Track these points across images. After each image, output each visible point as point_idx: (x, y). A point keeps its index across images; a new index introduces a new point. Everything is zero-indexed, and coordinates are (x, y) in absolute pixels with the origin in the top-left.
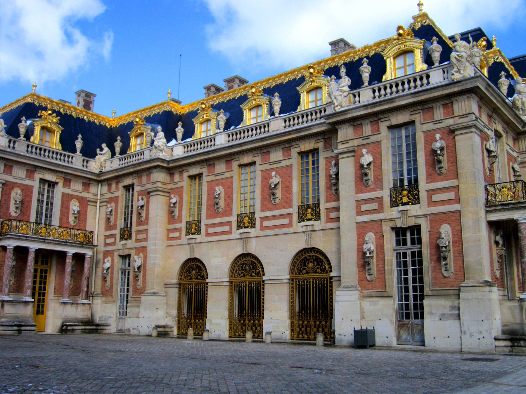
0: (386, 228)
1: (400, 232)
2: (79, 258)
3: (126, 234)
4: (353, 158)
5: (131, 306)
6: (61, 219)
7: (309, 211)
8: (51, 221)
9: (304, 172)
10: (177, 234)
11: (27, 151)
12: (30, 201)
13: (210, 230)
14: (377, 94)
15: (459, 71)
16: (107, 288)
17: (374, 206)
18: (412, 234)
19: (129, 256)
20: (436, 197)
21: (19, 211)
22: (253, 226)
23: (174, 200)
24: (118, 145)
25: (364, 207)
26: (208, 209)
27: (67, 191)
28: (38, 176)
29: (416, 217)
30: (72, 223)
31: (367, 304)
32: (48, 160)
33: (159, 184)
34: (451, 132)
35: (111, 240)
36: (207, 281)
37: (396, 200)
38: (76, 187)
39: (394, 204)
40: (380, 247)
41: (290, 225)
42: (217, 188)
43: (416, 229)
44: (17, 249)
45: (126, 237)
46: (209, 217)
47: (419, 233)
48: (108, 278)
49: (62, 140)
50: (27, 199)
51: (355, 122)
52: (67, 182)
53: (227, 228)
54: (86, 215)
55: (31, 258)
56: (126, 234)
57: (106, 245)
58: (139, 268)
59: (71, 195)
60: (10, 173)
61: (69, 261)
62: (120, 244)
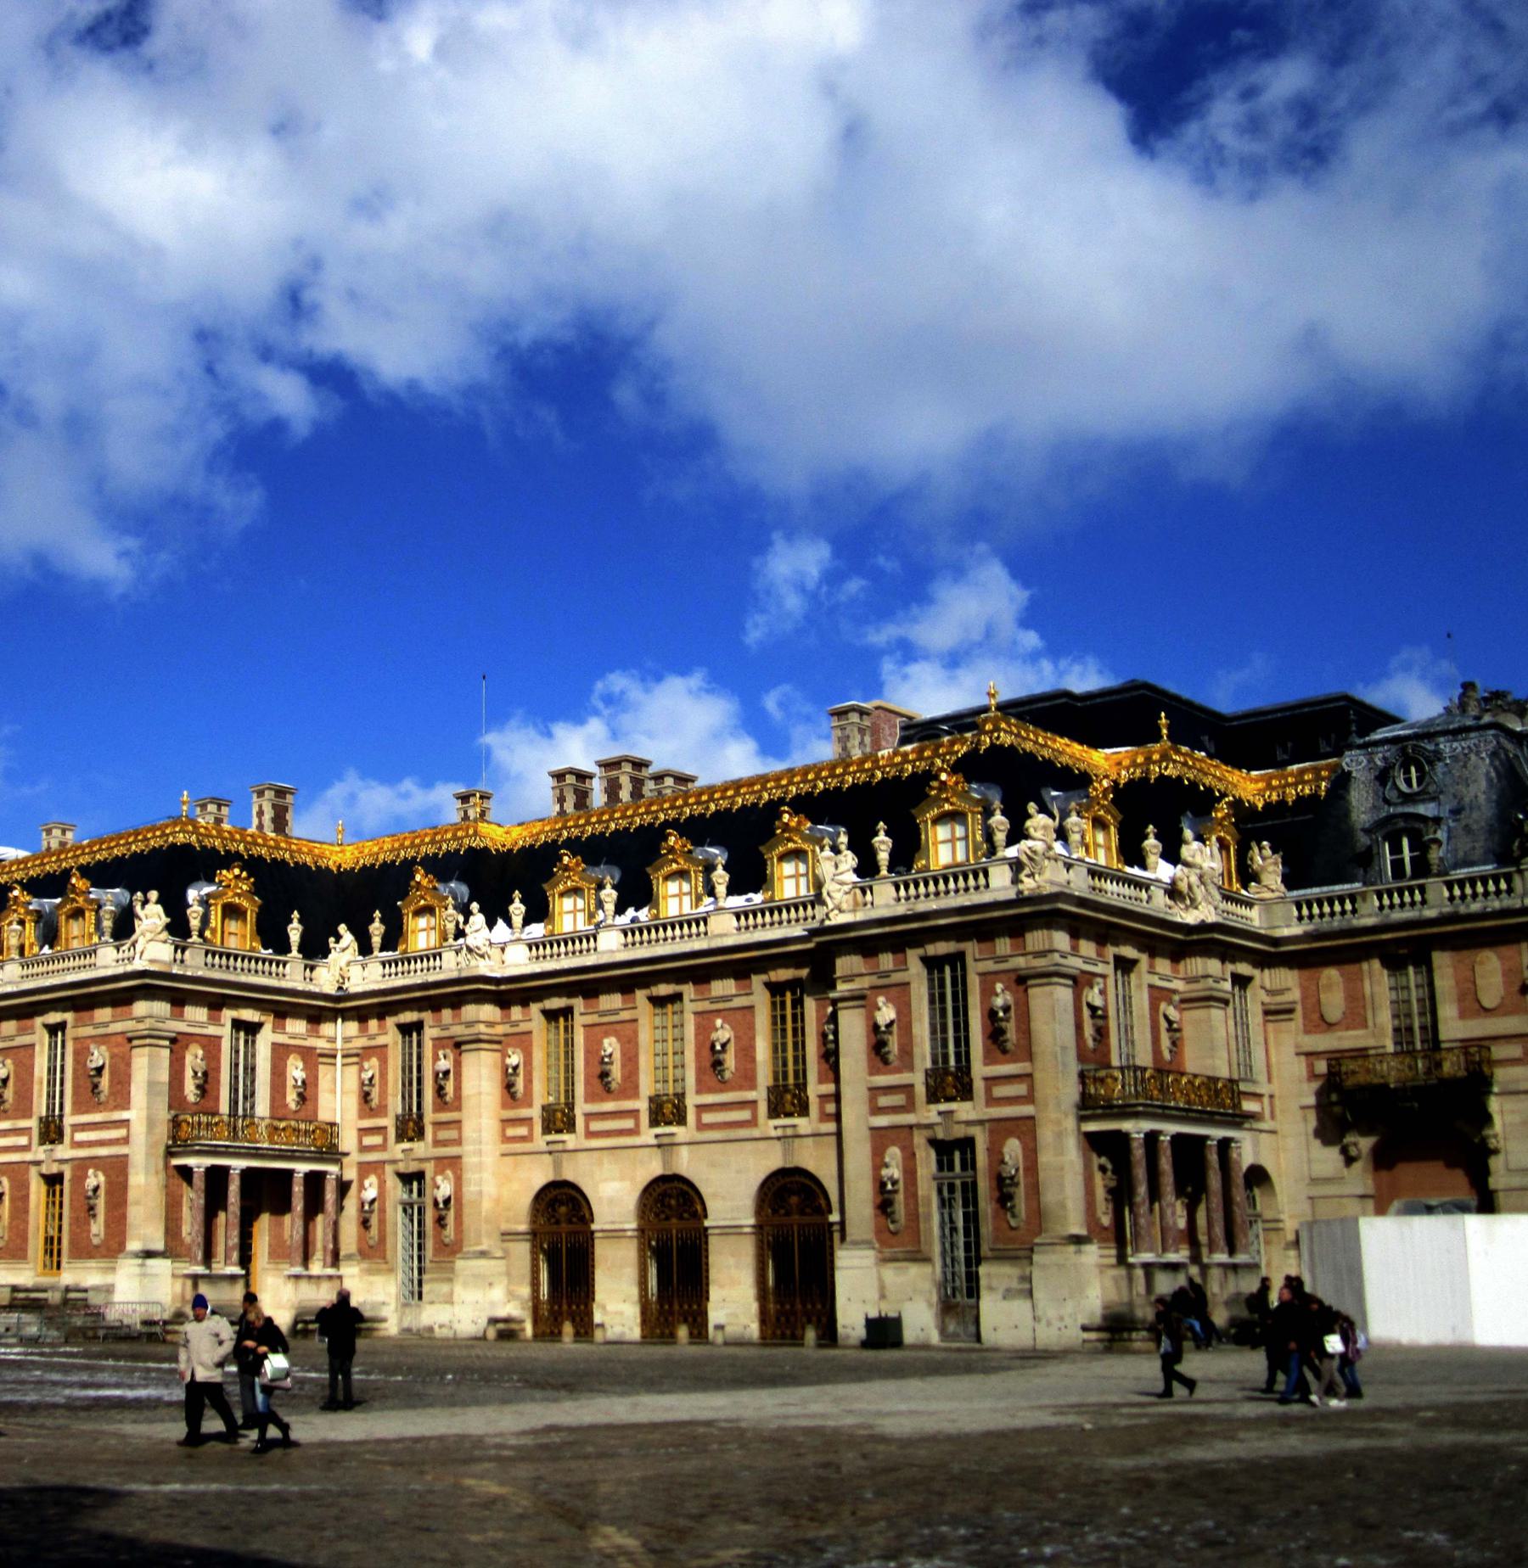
0: (919, 1139)
1: (943, 1149)
2: (315, 1182)
3: (410, 1128)
4: (862, 1011)
5: (432, 1280)
7: (787, 1099)
8: (252, 1107)
9: (778, 1021)
12: (218, 1069)
13: (596, 1126)
15: (1031, 875)
16: (371, 1242)
19: (419, 1176)
20: (1000, 1091)
22: (681, 1120)
24: (377, 929)
25: (884, 1101)
26: (587, 1083)
27: (281, 1039)
29: (968, 1123)
31: (890, 1273)
32: (243, 979)
33: (482, 1028)
34: (1022, 981)
35: (376, 1140)
40: (910, 1172)
41: (752, 1123)
42: (606, 1042)
43: (967, 1144)
45: (411, 1133)
48: (374, 1220)
50: (213, 1065)
53: (628, 1124)
54: (316, 1085)
55: (234, 1188)
58: (447, 1201)
60: (179, 1016)
61: (298, 1189)
62: (397, 1150)
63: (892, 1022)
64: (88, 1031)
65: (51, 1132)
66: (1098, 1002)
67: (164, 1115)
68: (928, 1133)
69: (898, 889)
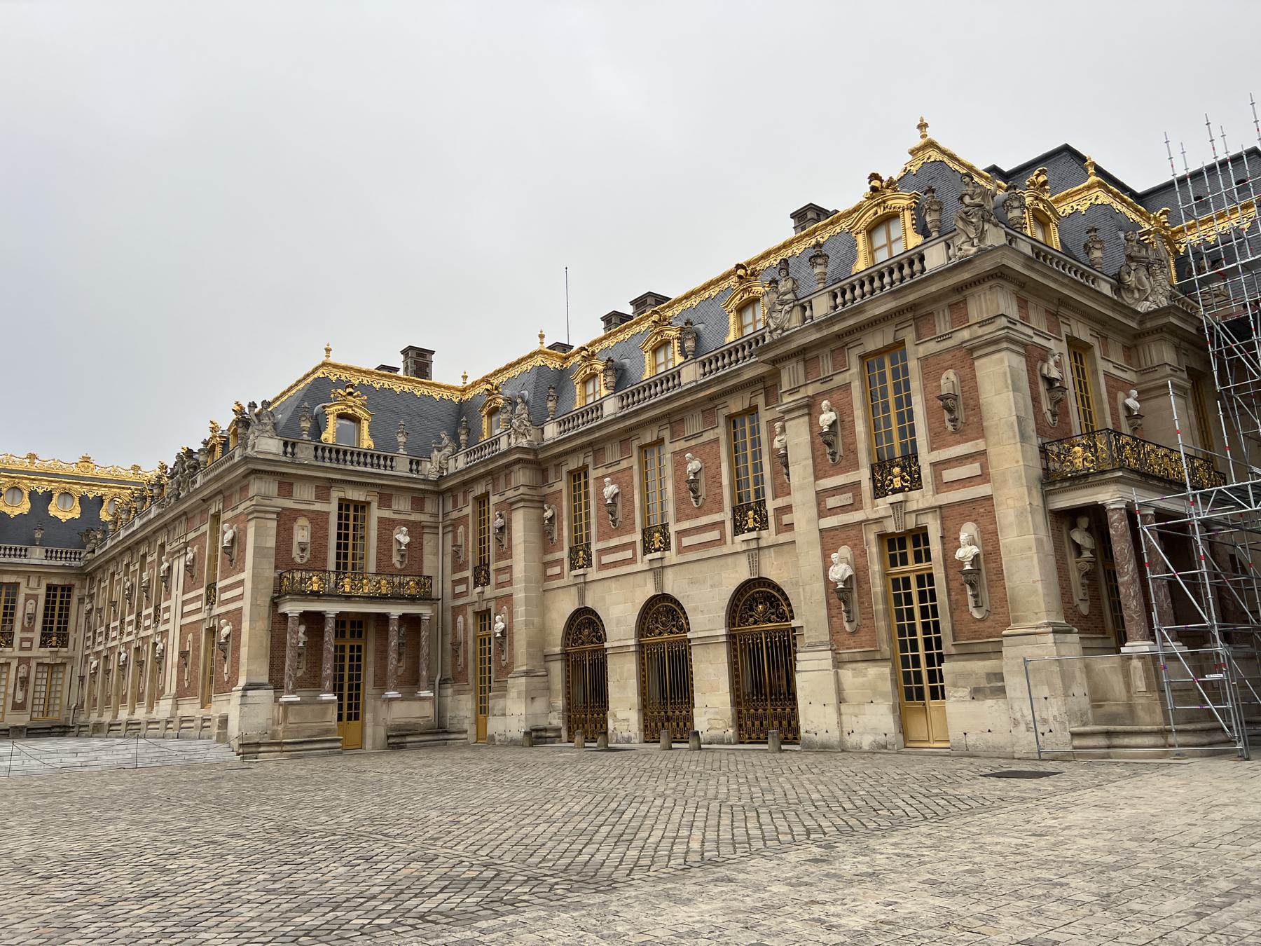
0: (871, 536)
2: (411, 622)
6: (379, 561)
10: (557, 570)
11: (316, 457)
12: (326, 537)
13: (606, 559)
14: (839, 300)
17: (845, 499)
18: (916, 544)
20: (949, 475)
21: (307, 555)
23: (548, 514)
25: (832, 502)
26: (599, 524)
27: (386, 514)
28: (336, 495)
29: (919, 512)
30: (398, 565)
32: (351, 468)
36: (606, 645)
37: (883, 486)
38: (402, 505)
39: (880, 491)
43: (920, 536)
44: (305, 617)
47: (927, 542)
49: (372, 435)
50: (320, 533)
51: (805, 354)
52: (385, 501)
53: (628, 554)
54: (421, 550)
55: (330, 627)
56: (481, 575)
57: (456, 596)
59: (394, 520)
60: (289, 495)
63: (835, 422)
64: (229, 515)
66: (1055, 374)
67: (270, 573)
68: (876, 529)
69: (835, 297)
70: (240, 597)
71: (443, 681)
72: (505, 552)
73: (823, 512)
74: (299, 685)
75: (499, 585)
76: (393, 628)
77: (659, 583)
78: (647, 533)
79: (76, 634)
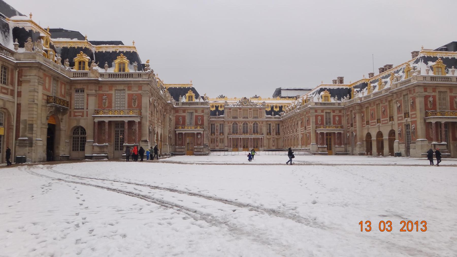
13: (372, 124)
27: (334, 114)
38: (337, 113)
46: (371, 120)
52: (334, 112)
53: (375, 124)
55: (325, 135)
56: (352, 125)
57: (348, 129)
65: (305, 129)
67: (315, 126)
70: (310, 130)
71: (346, 144)
72: (355, 122)
73: (398, 120)
74: (321, 144)
75: (355, 128)
76: (336, 135)
77: (379, 129)
78: (378, 120)
79: (281, 133)
